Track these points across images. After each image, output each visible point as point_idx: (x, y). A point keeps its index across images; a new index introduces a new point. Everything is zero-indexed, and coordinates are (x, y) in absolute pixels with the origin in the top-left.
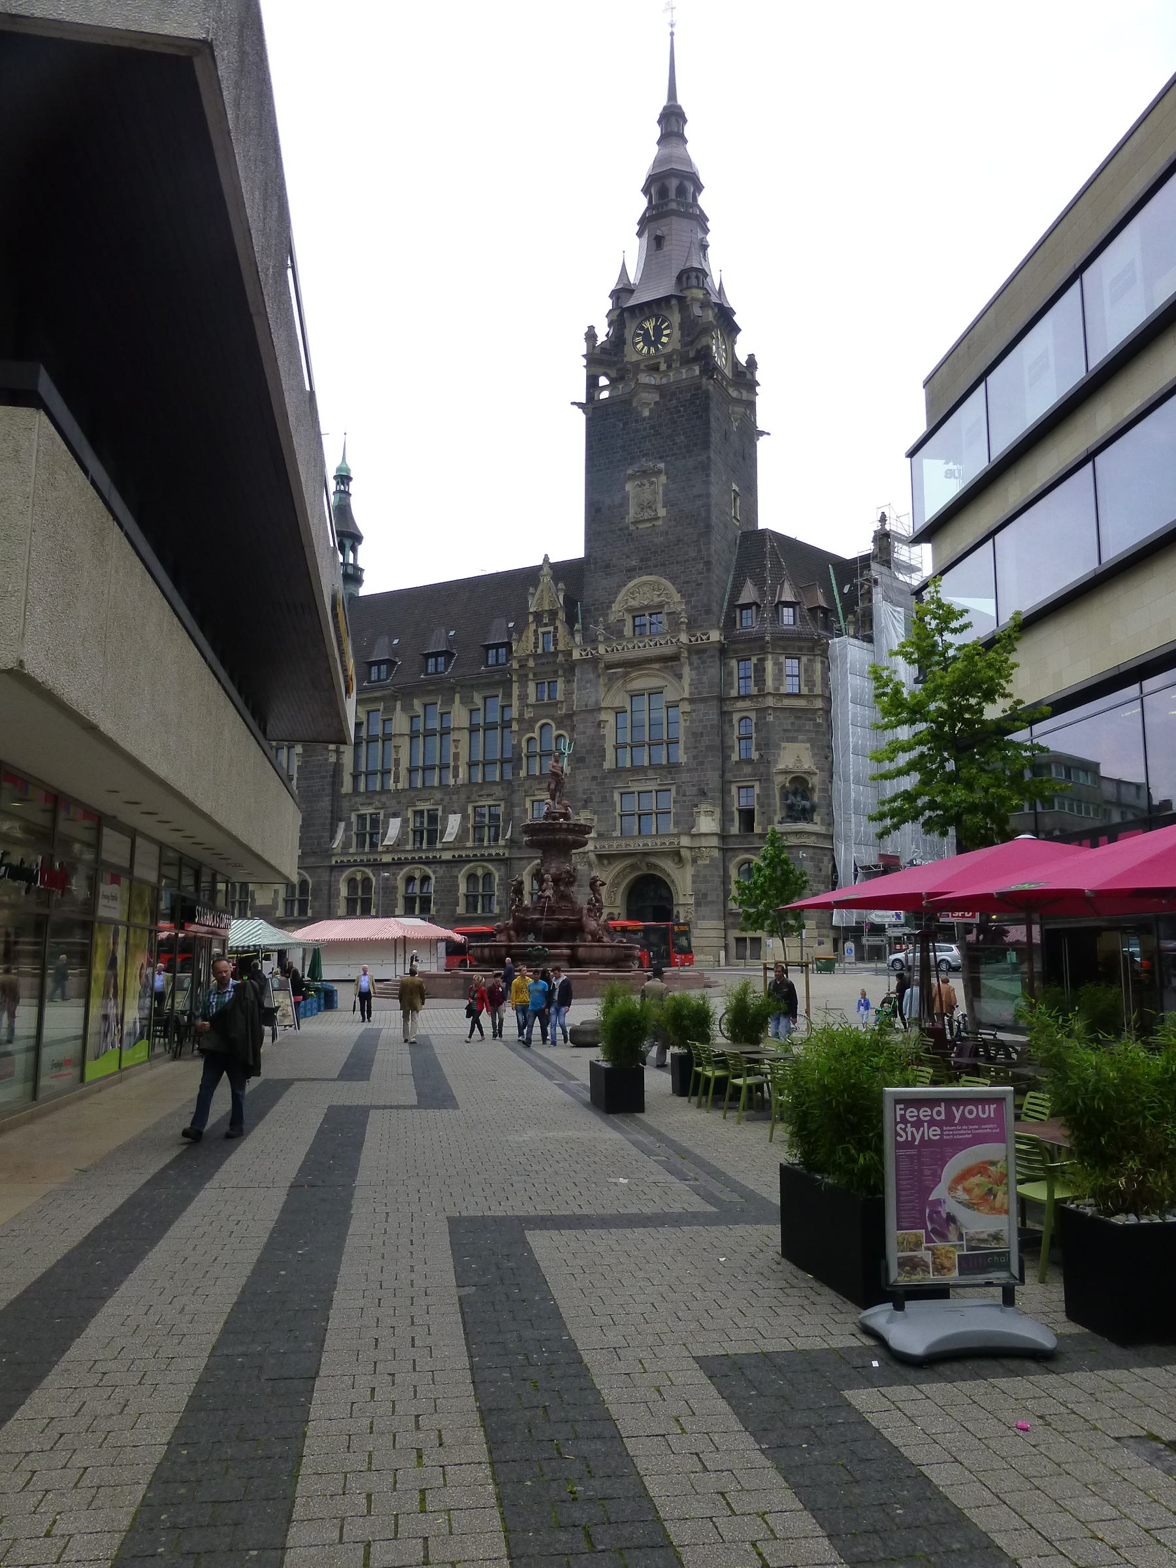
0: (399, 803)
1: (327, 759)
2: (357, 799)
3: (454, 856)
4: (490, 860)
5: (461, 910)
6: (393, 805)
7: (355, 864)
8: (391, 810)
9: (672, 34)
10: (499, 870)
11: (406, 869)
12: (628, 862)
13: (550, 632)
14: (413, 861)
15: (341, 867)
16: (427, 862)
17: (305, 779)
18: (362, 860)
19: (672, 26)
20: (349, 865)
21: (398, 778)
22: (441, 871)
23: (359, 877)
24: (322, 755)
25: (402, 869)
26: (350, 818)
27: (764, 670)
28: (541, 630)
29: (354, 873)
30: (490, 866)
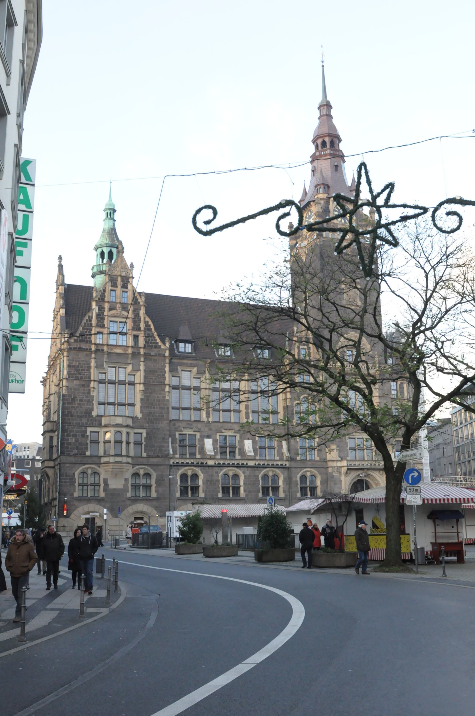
0: (210, 429)
1: (165, 397)
2: (180, 424)
3: (255, 464)
4: (277, 467)
5: (220, 495)
6: (206, 431)
7: (187, 465)
8: (205, 434)
9: (323, 66)
10: (283, 473)
11: (225, 470)
12: (359, 472)
13: (305, 349)
14: (229, 465)
15: (178, 465)
16: (238, 466)
17: (148, 407)
18: (198, 463)
19: (323, 62)
20: (183, 465)
21: (209, 414)
22: (248, 472)
23: (190, 473)
24: (160, 394)
25: (222, 470)
26: (175, 435)
27: (403, 388)
28: (301, 347)
29: (186, 470)
30: (278, 471)
